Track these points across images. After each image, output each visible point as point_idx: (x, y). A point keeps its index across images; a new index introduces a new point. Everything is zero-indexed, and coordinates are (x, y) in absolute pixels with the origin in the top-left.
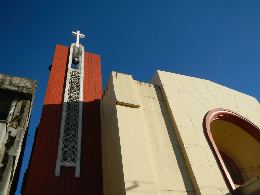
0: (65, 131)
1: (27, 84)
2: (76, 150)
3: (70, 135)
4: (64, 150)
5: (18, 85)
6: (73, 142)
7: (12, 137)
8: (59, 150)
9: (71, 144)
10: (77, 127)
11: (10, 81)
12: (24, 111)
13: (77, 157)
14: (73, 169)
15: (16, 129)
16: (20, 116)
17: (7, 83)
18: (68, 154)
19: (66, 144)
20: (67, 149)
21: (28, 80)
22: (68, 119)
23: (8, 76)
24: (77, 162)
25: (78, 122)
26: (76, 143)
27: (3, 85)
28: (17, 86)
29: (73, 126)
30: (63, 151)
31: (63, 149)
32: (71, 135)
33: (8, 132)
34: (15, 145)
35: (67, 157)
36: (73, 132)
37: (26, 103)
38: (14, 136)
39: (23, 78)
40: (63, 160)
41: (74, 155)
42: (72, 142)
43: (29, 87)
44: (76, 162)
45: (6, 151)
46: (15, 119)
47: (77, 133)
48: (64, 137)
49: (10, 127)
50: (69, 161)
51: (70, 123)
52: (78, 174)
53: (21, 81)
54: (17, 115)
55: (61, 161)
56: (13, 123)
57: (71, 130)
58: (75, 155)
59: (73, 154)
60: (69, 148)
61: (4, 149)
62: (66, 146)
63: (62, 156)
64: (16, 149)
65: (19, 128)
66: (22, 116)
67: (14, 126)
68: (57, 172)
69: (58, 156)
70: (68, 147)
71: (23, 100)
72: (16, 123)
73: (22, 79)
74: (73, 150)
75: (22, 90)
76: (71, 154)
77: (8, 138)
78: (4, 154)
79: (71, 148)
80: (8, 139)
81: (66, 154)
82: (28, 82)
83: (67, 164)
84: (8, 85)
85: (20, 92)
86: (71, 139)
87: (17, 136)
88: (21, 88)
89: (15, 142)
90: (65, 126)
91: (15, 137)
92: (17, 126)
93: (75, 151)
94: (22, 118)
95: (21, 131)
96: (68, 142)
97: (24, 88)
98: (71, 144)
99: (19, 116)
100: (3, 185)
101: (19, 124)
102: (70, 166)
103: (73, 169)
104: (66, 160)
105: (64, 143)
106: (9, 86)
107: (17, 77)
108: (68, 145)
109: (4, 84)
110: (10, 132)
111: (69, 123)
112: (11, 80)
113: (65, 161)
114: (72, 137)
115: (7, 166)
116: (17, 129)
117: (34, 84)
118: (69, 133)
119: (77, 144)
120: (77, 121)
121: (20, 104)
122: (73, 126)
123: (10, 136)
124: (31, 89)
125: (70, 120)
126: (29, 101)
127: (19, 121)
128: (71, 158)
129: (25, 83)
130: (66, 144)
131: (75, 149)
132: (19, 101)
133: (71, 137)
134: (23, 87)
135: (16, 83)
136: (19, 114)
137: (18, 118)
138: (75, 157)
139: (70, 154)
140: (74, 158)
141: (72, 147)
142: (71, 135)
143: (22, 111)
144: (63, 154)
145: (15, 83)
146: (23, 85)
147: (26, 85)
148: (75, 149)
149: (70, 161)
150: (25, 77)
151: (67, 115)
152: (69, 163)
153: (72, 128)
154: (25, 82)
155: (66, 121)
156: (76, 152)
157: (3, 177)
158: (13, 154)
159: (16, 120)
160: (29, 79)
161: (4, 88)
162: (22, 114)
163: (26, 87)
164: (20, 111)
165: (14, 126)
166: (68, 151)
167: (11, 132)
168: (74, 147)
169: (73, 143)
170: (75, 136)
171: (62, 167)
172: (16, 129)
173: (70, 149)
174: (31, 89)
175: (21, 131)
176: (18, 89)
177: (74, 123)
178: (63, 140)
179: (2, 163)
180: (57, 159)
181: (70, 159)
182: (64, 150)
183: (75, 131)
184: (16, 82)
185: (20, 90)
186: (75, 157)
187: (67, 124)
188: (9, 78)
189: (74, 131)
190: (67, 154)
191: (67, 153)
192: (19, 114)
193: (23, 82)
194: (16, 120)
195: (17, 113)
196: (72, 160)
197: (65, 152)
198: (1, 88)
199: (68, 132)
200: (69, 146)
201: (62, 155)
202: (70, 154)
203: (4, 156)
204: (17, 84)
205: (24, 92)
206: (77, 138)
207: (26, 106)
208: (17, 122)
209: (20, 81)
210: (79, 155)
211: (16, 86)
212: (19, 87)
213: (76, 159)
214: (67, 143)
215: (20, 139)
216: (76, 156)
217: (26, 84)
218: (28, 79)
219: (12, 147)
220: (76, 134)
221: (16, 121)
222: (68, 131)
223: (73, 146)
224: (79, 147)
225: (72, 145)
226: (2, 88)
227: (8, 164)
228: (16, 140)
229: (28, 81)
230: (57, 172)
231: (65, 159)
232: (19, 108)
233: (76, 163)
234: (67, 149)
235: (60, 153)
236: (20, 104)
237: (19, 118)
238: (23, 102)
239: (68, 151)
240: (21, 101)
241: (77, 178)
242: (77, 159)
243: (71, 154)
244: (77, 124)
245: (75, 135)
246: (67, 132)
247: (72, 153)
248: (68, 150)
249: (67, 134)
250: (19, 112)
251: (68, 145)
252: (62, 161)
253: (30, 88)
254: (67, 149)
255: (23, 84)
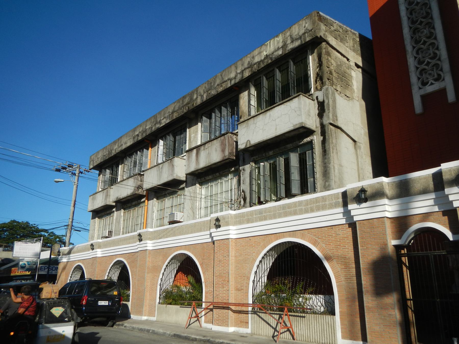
0: (412, 38)
1: (306, 25)
2: (439, 59)
3: (422, 39)
4: (419, 70)
5: (299, 34)
6: (431, 48)
7: (321, 102)
8: (410, 74)
9: (427, 55)
10: (432, 18)
11: (291, 36)
12: (322, 62)
13: (443, 70)
14: (443, 91)
15: (321, 90)
16: (320, 71)
17: (289, 41)
18: (427, 74)
19: (420, 58)
20: (423, 66)
21: (306, 18)
22: (411, 14)
23: (286, 31)
24: (446, 79)
25: (430, 8)
26: (436, 47)
27: (287, 47)
28: (299, 37)
29: (423, 20)
30: (418, 73)
31: (417, 68)
32: (424, 39)
33: (315, 98)
34: (326, 110)
35: (427, 79)
36: (425, 31)
37: (321, 49)
38: (322, 101)
39: (301, 20)
40: (421, 86)
41: (437, 69)
42: (429, 49)
43: (310, 28)
44: (444, 80)
45: (320, 121)
46: (317, 78)
47: (434, 28)
48: (414, 47)
49: (315, 91)
50: (432, 84)
51: (417, 17)
52: (451, 97)
53: (300, 28)
54: (317, 72)
55: (418, 89)
56: (317, 84)
57: (421, 31)
58: (440, 69)
59: (435, 70)
60: (425, 63)
61: (318, 119)
62: (420, 63)
63: (418, 81)
64: (329, 115)
65: (324, 87)
66: (322, 70)
67: (319, 88)
68: (418, 107)
69: (411, 84)
70: (424, 62)
71: (316, 47)
72: (320, 83)
73: (301, 22)
74: (433, 62)
75: (305, 39)
76: (433, 71)
77: (317, 106)
78: (320, 125)
79: (429, 61)
80: (318, 107)
81: (424, 75)
82: (306, 23)
83: (429, 89)
84: (291, 43)
85: (304, 43)
86: (425, 45)
87: (325, 99)
88: (303, 38)
89: (326, 108)
90: (410, 28)
91: (324, 101)
92: (321, 86)
93: (438, 63)
94: (323, 73)
95: (326, 91)
96: (422, 52)
97: (306, 34)
98: (427, 55)
99: (319, 72)
100: (329, 158)
101: (322, 83)
102: (434, 90)
103: (443, 91)
104: (427, 83)
105: (415, 58)
106: (292, 43)
107: (295, 24)
108: (423, 57)
109: (287, 45)
110: (317, 98)
111: (414, 20)
112: (291, 35)
113: (424, 87)
114: (427, 40)
115: (327, 137)
116: (322, 90)
117: (313, 18)
118: (420, 37)
119: (437, 49)
120: (428, 7)
121: (315, 54)
122: (423, 20)
123: (318, 102)
124: (312, 29)
125: (415, 12)
126: (323, 43)
127: (321, 79)
128: (434, 76)
129: (305, 27)
130: (420, 58)
131: (438, 58)
132: (312, 53)
133: (425, 43)
134: (304, 34)
135: (296, 35)
136: (318, 69)
137: (319, 74)
138: (440, 73)
139: (430, 72)
140: (439, 76)
141: (431, 58)
142: (424, 39)
143: (320, 63)
144: (419, 76)
145: (295, 35)
146: (302, 31)
147: (307, 28)
148: (436, 59)
149: (433, 82)
150: (301, 18)
151: (408, 7)
152: (433, 85)
153: (423, 24)
154: (304, 26)
155: (409, 18)
156: (439, 62)
157: (327, 150)
158: (328, 122)
159: (318, 79)
160: (307, 16)
161: (288, 50)
162: (322, 68)
163: (308, 31)
164: (318, 65)
165: (319, 88)
166: (426, 67)
167: (318, 97)
168: (435, 56)
169: (431, 51)
170: (432, 35)
171: (424, 98)
172: (321, 90)
173: (428, 63)
174: (312, 29)
175: (326, 91)
176: (301, 41)
177: (423, 14)
178: (412, 54)
179: (321, 135)
180: (412, 89)
181: (432, 79)
182: (419, 70)
183: (429, 27)
184: (296, 33)
185: (303, 40)
186: (440, 73)
187: (413, 22)
188: (288, 34)
189: (427, 29)
190: (426, 73)
191: (424, 72)
192: (319, 70)
193: (302, 26)
194: (318, 79)
195: (316, 70)
196: (436, 80)
197: (422, 72)
198: (286, 53)
199: (417, 36)
200: (425, 58)
201: (419, 79)
202: (430, 72)
203: (321, 128)
204: (298, 34)
205: (308, 39)
206: (435, 38)
207: (322, 53)
208: (320, 82)
209: (299, 28)
210: (446, 66)
211: (297, 39)
212: (300, 38)
213: (442, 75)
214: (420, 56)
215: (328, 101)
216: (441, 70)
217: (306, 27)
218: (305, 18)
219: (325, 114)
220: (432, 31)
221: (319, 81)
222: (417, 34)
223: (432, 55)
224: (443, 52)
225: (430, 54)
226: (287, 52)
227: (326, 134)
228: (325, 104)
229: (307, 21)
230: (418, 107)
231: (424, 84)
232: (316, 62)
233: (444, 81)
234: (423, 65)
235: (414, 78)
236: (315, 54)
237: (320, 74)
238: (318, 51)
239: (426, 67)
240: (316, 51)
241: (453, 104)
242: (444, 74)
243: (433, 71)
244: (430, 12)
245: (431, 34)
246: (416, 37)
247: (433, 68)
248: (425, 66)
249: (417, 42)
250: (317, 68)
251: (423, 59)
252: (420, 88)
253: (312, 28)
254: (423, 66)
255: (302, 29)
